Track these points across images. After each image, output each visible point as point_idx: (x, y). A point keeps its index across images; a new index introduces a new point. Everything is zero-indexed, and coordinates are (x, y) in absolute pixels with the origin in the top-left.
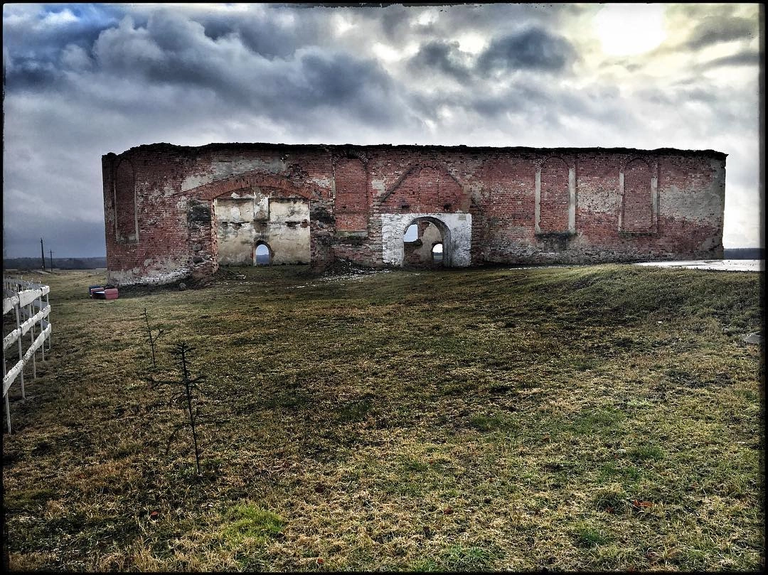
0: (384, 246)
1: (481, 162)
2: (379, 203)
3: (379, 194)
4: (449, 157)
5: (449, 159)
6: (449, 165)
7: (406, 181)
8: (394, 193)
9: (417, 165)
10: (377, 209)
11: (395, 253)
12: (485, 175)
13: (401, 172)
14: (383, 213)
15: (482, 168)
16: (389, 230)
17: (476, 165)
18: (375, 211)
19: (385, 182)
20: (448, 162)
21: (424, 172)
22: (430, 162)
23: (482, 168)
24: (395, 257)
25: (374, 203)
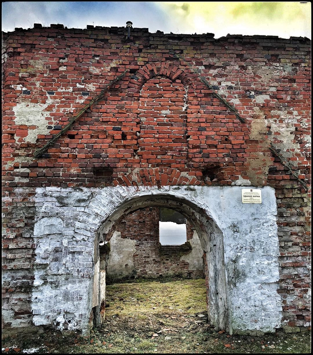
0: (37, 274)
1: (289, 69)
2: (30, 160)
3: (31, 137)
4: (212, 55)
5: (212, 61)
6: (213, 72)
7: (104, 107)
8: (72, 137)
9: (133, 71)
10: (24, 176)
11: (67, 297)
12: (301, 97)
13: (91, 87)
14: (41, 186)
15: (292, 81)
16: (54, 230)
17: (276, 74)
18: (17, 179)
19: (50, 108)
20: (209, 67)
21: (150, 89)
22: (164, 67)
23: (294, 81)
24: (68, 306)
25: (17, 160)
